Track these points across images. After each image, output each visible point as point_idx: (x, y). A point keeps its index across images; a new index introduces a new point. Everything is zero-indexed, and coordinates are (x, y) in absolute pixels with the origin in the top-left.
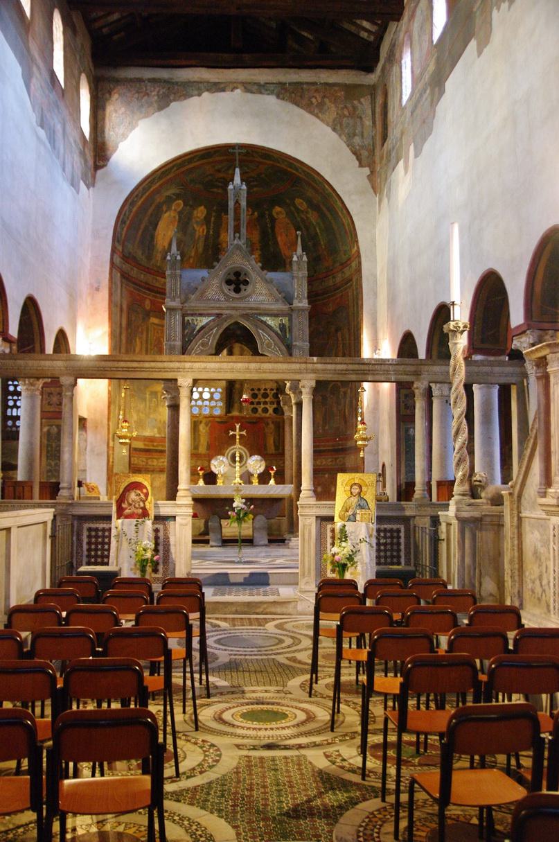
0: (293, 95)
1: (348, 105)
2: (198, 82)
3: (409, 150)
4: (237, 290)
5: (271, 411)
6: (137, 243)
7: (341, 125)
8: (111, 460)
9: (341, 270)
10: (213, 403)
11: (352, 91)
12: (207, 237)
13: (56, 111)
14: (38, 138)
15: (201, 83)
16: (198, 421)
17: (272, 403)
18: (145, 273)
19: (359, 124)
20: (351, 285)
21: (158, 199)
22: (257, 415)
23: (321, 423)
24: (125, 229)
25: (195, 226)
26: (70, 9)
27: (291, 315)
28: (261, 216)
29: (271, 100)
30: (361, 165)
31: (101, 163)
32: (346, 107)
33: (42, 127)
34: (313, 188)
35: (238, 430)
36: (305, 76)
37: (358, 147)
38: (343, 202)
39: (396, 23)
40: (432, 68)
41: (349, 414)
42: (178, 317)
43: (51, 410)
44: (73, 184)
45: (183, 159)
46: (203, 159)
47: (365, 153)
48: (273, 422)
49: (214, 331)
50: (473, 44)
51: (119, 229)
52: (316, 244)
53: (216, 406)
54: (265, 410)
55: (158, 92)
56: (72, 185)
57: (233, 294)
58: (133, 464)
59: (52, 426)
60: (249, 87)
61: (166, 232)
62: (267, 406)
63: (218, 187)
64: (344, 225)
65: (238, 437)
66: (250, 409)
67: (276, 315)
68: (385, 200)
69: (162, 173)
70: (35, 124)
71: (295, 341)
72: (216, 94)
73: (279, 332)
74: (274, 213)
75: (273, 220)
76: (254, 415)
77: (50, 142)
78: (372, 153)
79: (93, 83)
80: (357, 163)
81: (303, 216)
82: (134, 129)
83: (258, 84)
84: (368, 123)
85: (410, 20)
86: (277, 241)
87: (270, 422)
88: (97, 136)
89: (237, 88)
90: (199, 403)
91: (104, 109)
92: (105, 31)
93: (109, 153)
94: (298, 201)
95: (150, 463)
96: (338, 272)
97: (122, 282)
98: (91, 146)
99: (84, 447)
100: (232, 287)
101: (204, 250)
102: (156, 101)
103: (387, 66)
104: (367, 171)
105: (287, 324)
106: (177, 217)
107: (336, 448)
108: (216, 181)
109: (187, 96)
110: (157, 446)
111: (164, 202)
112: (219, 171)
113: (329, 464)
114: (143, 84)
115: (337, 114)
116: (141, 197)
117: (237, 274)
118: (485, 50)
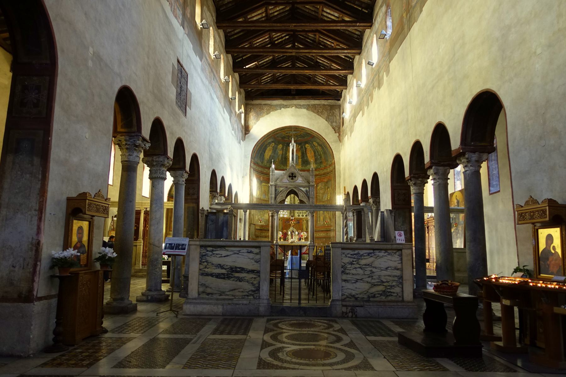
1: (331, 112)
2: (280, 105)
5: (305, 216)
7: (329, 119)
11: (332, 107)
12: (282, 155)
17: (305, 213)
21: (266, 143)
22: (300, 217)
23: (322, 220)
28: (302, 147)
29: (304, 111)
30: (335, 133)
31: (247, 132)
32: (330, 113)
34: (319, 139)
38: (329, 145)
40: (353, 112)
42: (274, 188)
44: (240, 143)
47: (337, 129)
51: (253, 155)
52: (321, 157)
54: (303, 216)
60: (297, 106)
61: (268, 154)
63: (286, 138)
67: (305, 187)
68: (343, 146)
75: (306, 149)
78: (339, 128)
84: (338, 118)
87: (304, 220)
91: (249, 115)
93: (250, 129)
94: (314, 143)
95: (262, 234)
98: (244, 127)
100: (291, 178)
104: (337, 134)
109: (276, 110)
111: (268, 144)
112: (287, 133)
117: (292, 174)
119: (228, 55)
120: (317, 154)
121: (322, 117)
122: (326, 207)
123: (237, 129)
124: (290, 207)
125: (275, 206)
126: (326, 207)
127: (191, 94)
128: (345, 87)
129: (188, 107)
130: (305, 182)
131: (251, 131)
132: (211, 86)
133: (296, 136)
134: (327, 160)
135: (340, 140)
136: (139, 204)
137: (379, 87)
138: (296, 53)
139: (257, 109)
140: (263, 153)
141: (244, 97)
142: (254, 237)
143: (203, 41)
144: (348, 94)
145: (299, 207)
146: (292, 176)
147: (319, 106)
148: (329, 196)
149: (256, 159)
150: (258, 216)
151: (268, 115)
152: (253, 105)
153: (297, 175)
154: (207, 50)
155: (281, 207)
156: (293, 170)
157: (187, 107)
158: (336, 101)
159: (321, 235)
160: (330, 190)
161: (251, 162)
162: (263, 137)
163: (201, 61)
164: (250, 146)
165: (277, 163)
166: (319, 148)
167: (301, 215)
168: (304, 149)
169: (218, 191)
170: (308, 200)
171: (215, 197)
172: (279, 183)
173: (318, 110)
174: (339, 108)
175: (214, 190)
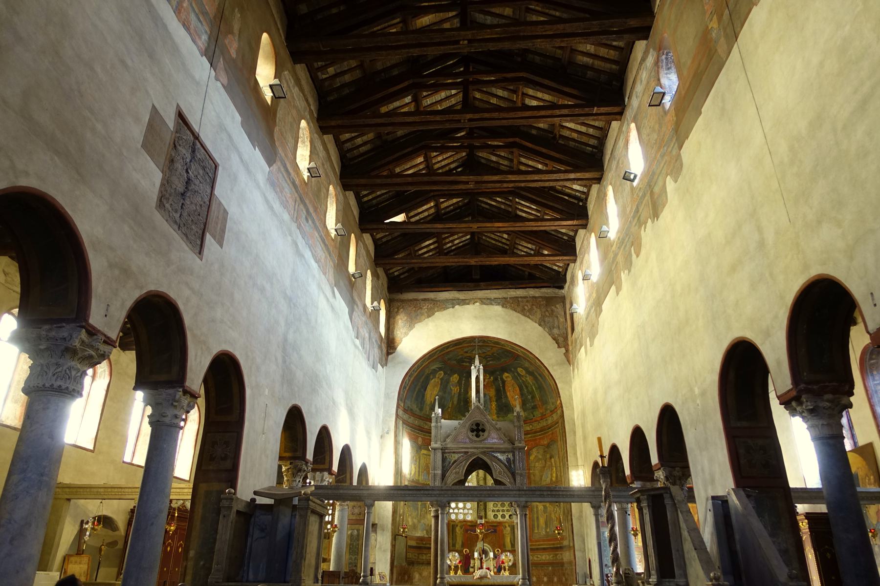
0: (512, 305)
1: (549, 309)
2: (452, 300)
3: (586, 341)
4: (478, 436)
5: (507, 517)
6: (413, 399)
7: (544, 322)
8: (393, 555)
9: (551, 415)
10: (466, 511)
11: (549, 301)
13: (366, 327)
14: (356, 346)
15: (454, 300)
16: (455, 525)
17: (508, 511)
18: (417, 419)
19: (556, 320)
20: (558, 426)
21: (427, 371)
22: (497, 520)
23: (544, 526)
24: (406, 392)
25: (452, 387)
26: (377, 267)
27: (514, 452)
28: (496, 379)
29: (498, 309)
31: (392, 351)
32: (547, 311)
33: (357, 338)
36: (520, 293)
37: (556, 336)
39: (573, 264)
40: (594, 295)
41: (563, 520)
42: (439, 455)
43: (354, 518)
44: (374, 367)
45: (443, 346)
46: (456, 346)
47: (561, 339)
48: (509, 526)
49: (463, 463)
50: (613, 288)
51: (402, 393)
52: (533, 397)
53: (468, 514)
54: (503, 516)
55: (428, 306)
56: (373, 368)
57: (475, 438)
58: (409, 558)
59: (354, 529)
60: (484, 301)
61: (432, 392)
62: (505, 513)
64: (550, 385)
67: (504, 452)
68: (576, 370)
69: (430, 356)
70: (353, 337)
71: (518, 470)
72: (463, 306)
73: (507, 464)
74: (504, 378)
75: (504, 382)
76: (495, 520)
77: (361, 346)
78: (567, 337)
79: (388, 303)
80: (557, 345)
81: (524, 379)
82: (412, 329)
83: (490, 299)
84: (562, 320)
85: (580, 264)
86: (507, 395)
87: (507, 525)
88: (389, 334)
89: (477, 302)
90: (456, 511)
92: (396, 274)
93: (396, 344)
94: (519, 370)
95: (421, 557)
96: (549, 416)
97: (403, 427)
98: (386, 341)
99: (375, 545)
100: (475, 433)
101: (458, 403)
102: (426, 312)
103: (571, 286)
104: (563, 350)
105: (512, 459)
106: (440, 382)
107: (555, 546)
108: (465, 358)
109: (445, 308)
110: (426, 544)
111: (431, 373)
112: (467, 352)
113: (552, 558)
114: (418, 302)
115: (542, 315)
116: (416, 372)
117: (478, 425)
118: (620, 293)
119: (347, 192)
120: (525, 390)
121: (532, 320)
122: (554, 493)
123: (367, 339)
124: (472, 492)
125: (438, 492)
126: (554, 493)
127: (226, 212)
128: (572, 258)
129: (214, 237)
130: (504, 442)
131: (398, 349)
132: (299, 228)
133: (484, 358)
134: (545, 402)
135: (568, 361)
136: (134, 490)
137: (656, 215)
138: (477, 182)
139: (410, 309)
140: (422, 390)
141: (386, 286)
142: (404, 564)
143: (277, 129)
144: (580, 269)
145: (493, 492)
146: (478, 429)
147: (525, 300)
148: (554, 475)
149: (408, 403)
150: (412, 518)
151: (430, 318)
152: (403, 301)
153: (487, 427)
154: (290, 155)
155: (449, 492)
156: (478, 418)
157: (208, 237)
158: (557, 291)
159: (544, 558)
160: (555, 461)
161: (398, 407)
162: (421, 359)
163: (270, 165)
164: (397, 375)
165: (449, 410)
166: (528, 379)
167: (500, 514)
168: (500, 382)
169: (310, 456)
170: (512, 481)
171: (300, 470)
172: (450, 444)
173: (523, 307)
174: (564, 302)
175: (299, 454)
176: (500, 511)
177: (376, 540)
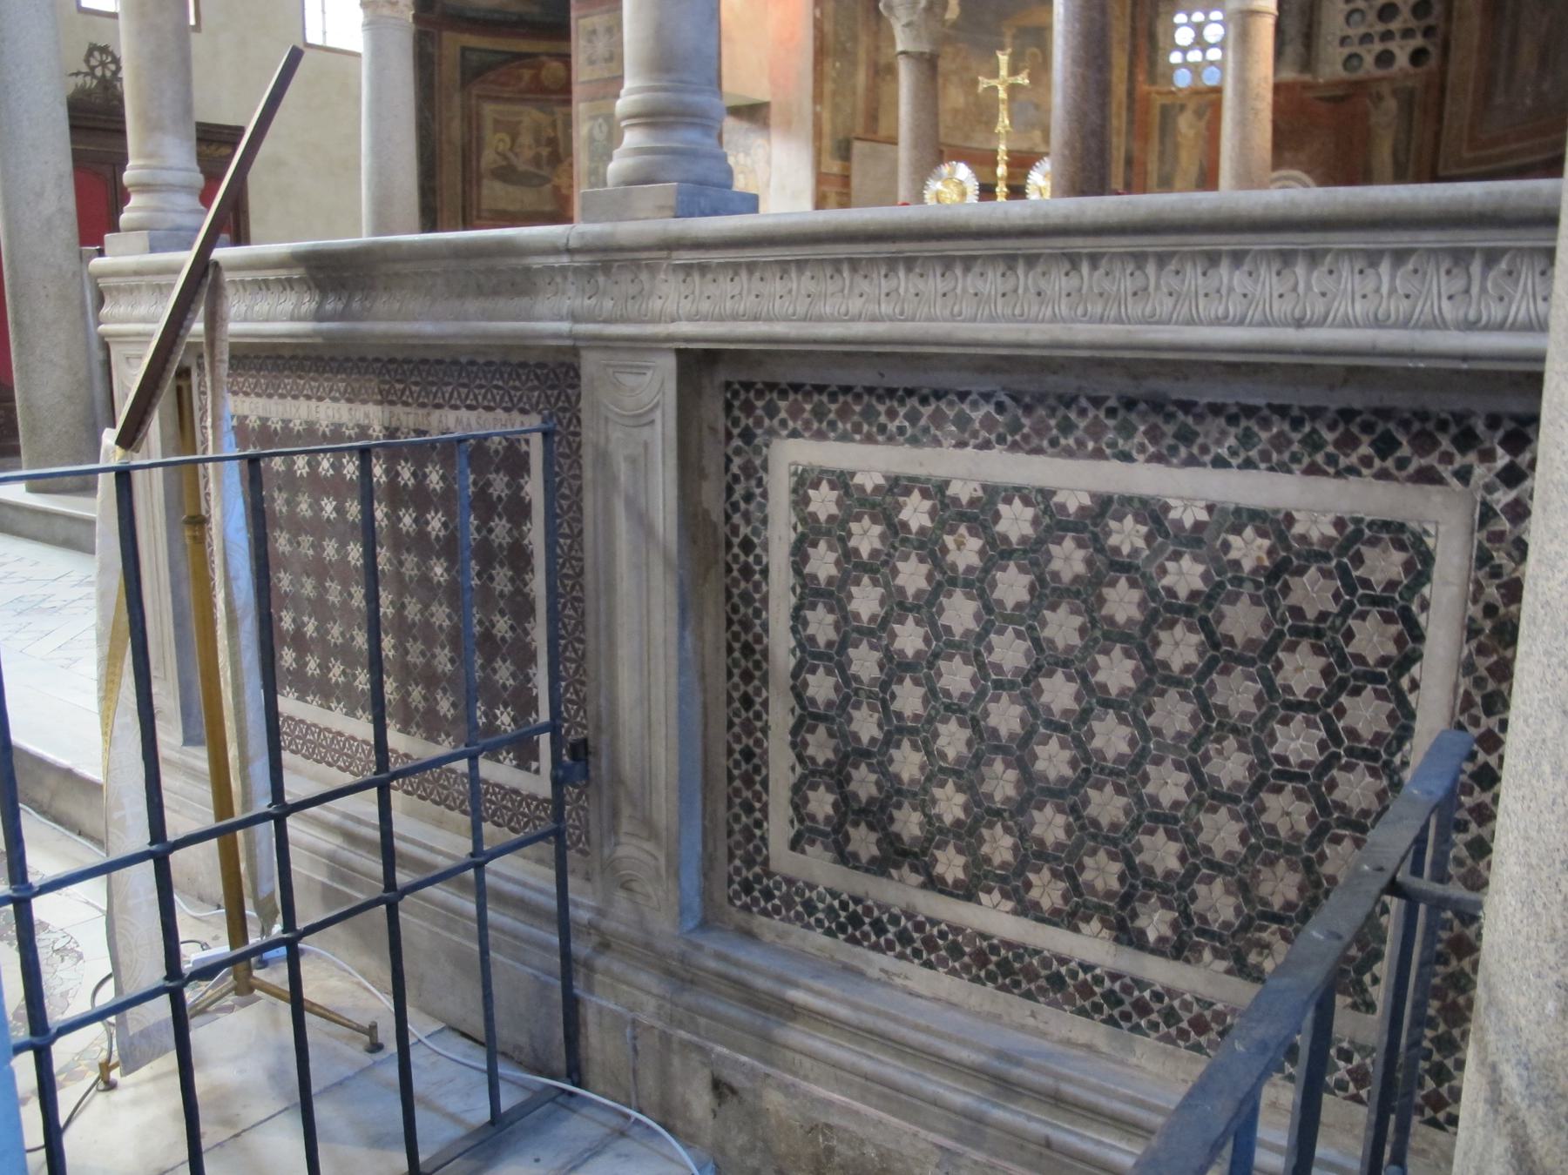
5: (1402, 60)
17: (1407, 33)
22: (1360, 74)
35: (1004, 72)
48: (1395, 93)
54: (1385, 59)
62: (1393, 46)
65: (1002, 95)
66: (1339, 60)
90: (1195, 56)
167: (1369, 55)
176: (1372, 41)
177: (769, 162)
